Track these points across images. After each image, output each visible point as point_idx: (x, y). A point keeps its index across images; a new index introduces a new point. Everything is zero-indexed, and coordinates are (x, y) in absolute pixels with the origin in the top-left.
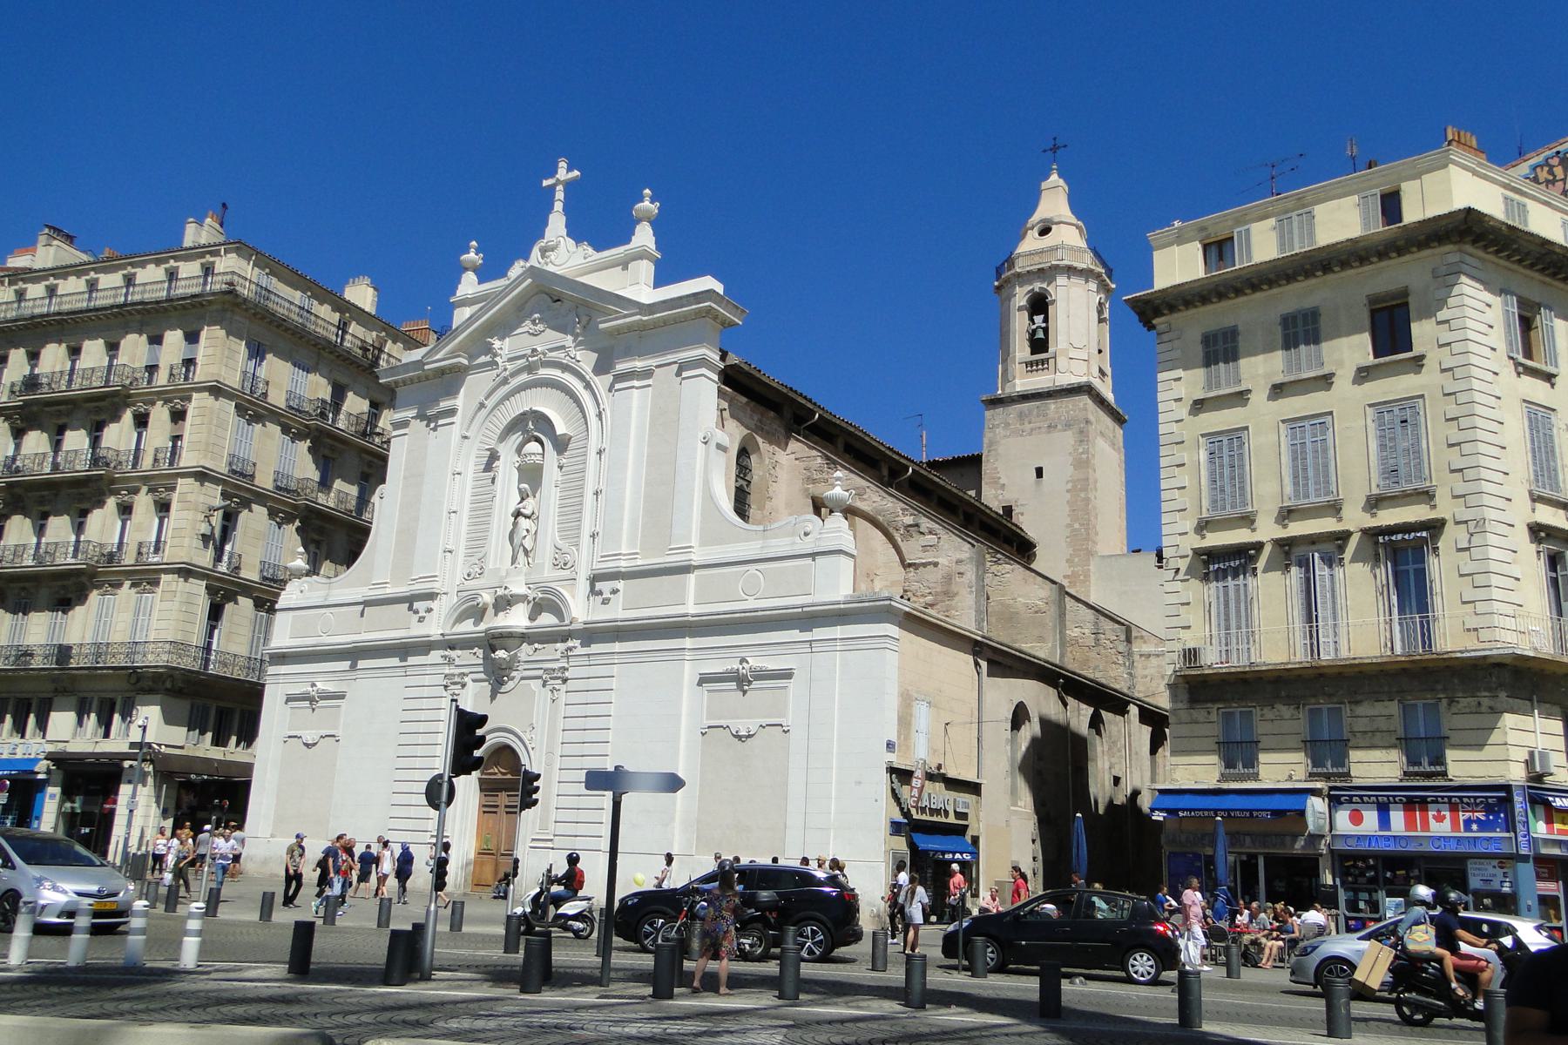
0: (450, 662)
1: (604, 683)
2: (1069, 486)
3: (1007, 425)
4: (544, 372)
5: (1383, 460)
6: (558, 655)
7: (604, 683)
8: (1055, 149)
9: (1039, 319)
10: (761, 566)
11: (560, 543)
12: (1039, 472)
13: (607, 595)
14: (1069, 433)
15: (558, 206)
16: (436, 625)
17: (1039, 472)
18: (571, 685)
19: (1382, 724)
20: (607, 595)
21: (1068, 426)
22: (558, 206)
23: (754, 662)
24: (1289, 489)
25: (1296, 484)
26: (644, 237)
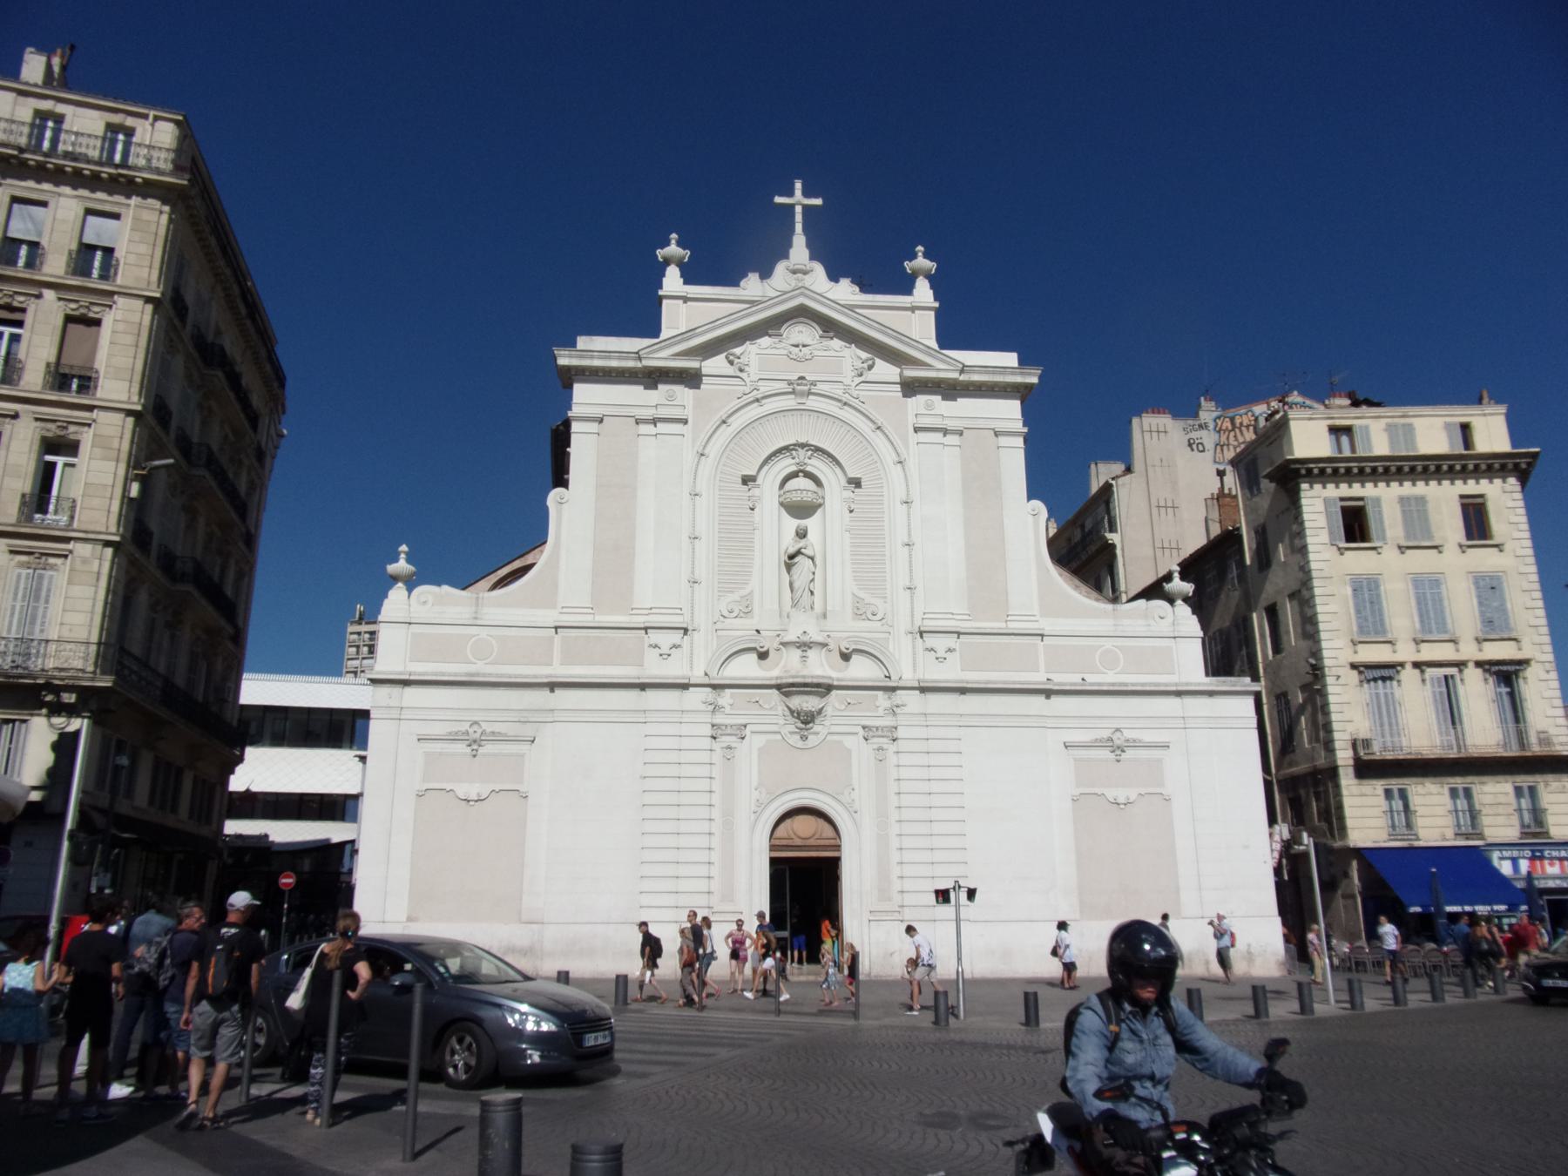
0: (716, 708)
1: (952, 746)
4: (813, 402)
5: (1482, 613)
6: (881, 712)
7: (952, 746)
10: (1120, 642)
11: (861, 594)
13: (941, 653)
15: (799, 227)
16: (694, 661)
19: (1502, 799)
22: (799, 227)
23: (1128, 734)
24: (1418, 625)
25: (1422, 622)
26: (923, 292)
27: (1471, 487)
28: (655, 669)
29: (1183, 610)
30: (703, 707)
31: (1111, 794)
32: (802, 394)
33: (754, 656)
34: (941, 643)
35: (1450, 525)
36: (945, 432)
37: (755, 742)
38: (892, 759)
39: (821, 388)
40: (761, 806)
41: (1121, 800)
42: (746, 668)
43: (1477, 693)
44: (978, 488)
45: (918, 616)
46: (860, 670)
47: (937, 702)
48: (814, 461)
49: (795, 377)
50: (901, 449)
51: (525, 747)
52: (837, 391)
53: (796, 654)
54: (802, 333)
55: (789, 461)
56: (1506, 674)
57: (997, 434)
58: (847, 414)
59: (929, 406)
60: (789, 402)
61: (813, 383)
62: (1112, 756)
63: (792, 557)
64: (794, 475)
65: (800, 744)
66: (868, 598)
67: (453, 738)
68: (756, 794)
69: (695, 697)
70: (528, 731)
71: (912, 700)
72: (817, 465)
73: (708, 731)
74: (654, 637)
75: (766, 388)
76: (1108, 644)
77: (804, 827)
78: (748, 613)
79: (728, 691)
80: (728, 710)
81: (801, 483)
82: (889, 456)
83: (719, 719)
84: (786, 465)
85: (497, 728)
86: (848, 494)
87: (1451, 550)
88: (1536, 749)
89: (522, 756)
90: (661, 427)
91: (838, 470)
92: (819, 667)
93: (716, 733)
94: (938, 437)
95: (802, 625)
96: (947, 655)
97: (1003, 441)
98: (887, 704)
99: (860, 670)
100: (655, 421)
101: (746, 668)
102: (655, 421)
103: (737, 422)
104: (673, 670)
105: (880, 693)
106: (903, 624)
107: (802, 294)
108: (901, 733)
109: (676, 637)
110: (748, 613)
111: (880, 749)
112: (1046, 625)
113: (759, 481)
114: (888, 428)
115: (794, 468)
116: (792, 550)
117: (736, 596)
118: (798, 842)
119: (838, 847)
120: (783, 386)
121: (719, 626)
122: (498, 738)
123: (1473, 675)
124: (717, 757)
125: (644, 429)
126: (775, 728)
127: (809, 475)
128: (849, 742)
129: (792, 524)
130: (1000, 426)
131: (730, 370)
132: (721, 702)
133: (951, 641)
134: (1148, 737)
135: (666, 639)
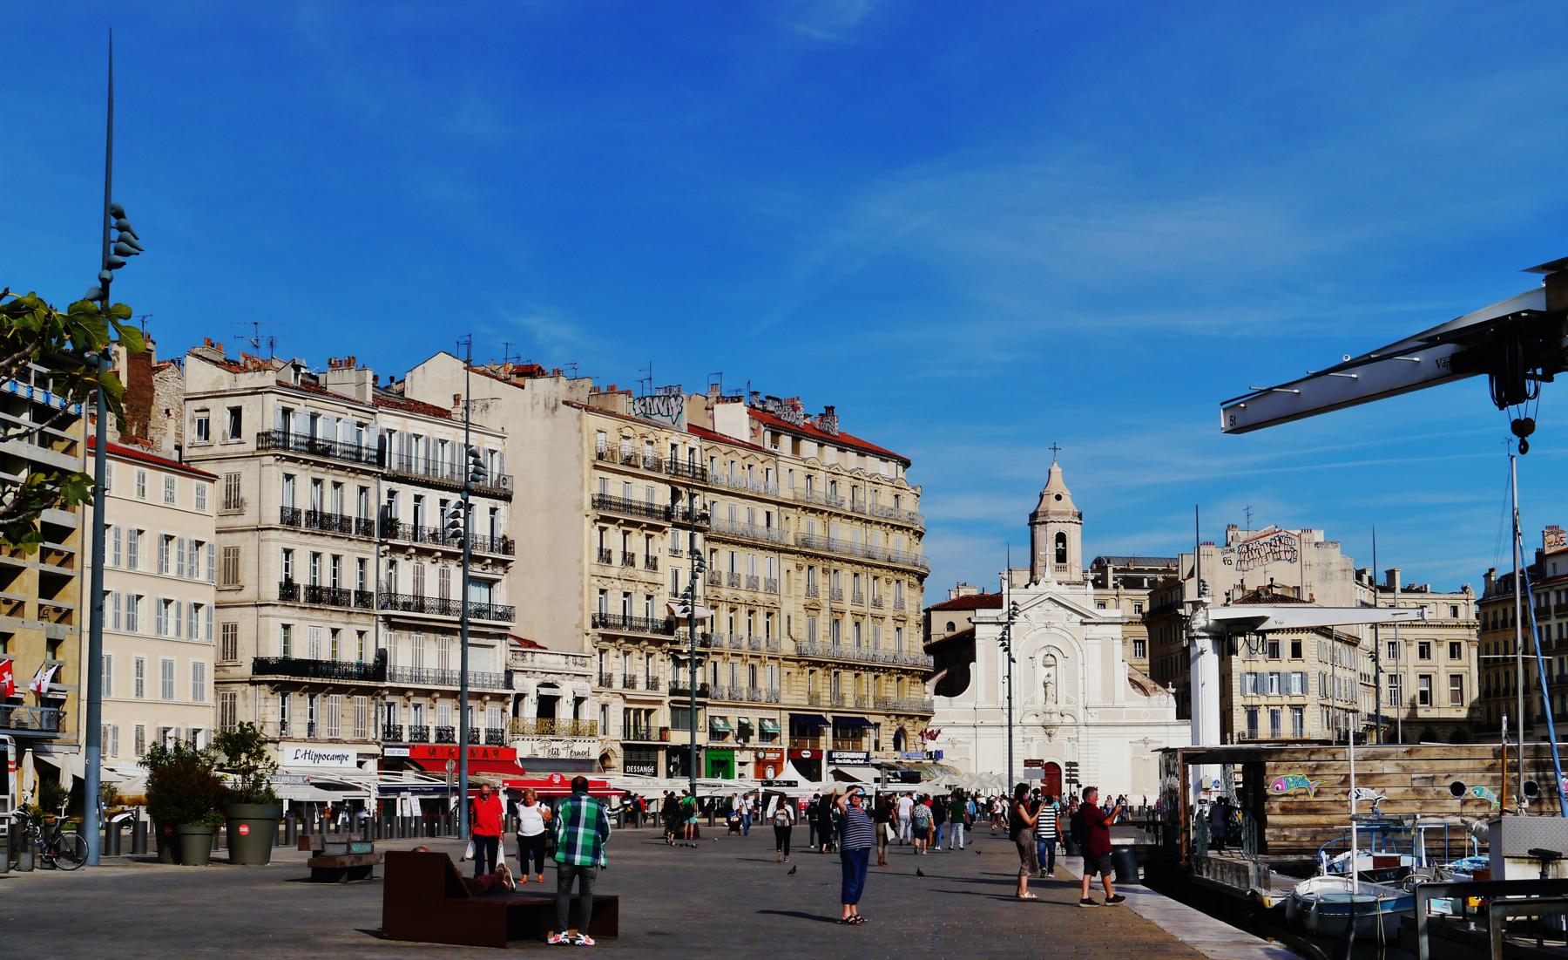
27: (1296, 636)
29: (1172, 698)
35: (1286, 650)
37: (1035, 743)
42: (1034, 720)
43: (1286, 717)
44: (1107, 659)
46: (1068, 720)
47: (1091, 730)
56: (1298, 709)
71: (1083, 729)
72: (1054, 652)
87: (1285, 661)
88: (1306, 736)
92: (1056, 719)
95: (1051, 706)
99: (1068, 720)
101: (1034, 720)
106: (1081, 705)
123: (1287, 709)
129: (1046, 671)
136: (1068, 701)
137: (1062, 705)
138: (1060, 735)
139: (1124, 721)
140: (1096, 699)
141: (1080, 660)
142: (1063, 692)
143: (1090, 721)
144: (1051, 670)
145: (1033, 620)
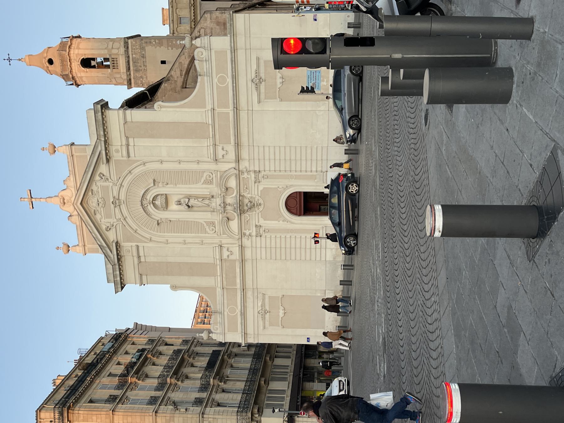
0: (250, 235)
2: (170, 48)
3: (142, 77)
4: (122, 197)
8: (9, 60)
9: (93, 63)
11: (202, 181)
12: (163, 62)
14: (146, 48)
17: (163, 62)
18: (262, 169)
20: (225, 152)
21: (143, 49)
23: (254, 75)
28: (236, 255)
30: (250, 240)
31: (279, 85)
32: (120, 202)
33: (231, 222)
34: (220, 153)
36: (128, 145)
37: (262, 222)
38: (267, 173)
39: (115, 194)
40: (285, 220)
41: (281, 80)
45: (209, 160)
46: (232, 183)
47: (245, 154)
48: (148, 198)
49: (112, 206)
50: (139, 163)
51: (267, 297)
52: (116, 189)
53: (228, 208)
54: (92, 203)
55: (149, 207)
57: (126, 122)
58: (125, 184)
59: (117, 151)
60: (123, 207)
61: (114, 197)
62: (263, 83)
63: (189, 206)
64: (154, 204)
65: (262, 206)
66: (204, 178)
67: (264, 319)
68: (281, 222)
69: (246, 242)
70: (260, 296)
71: (244, 165)
72: (150, 197)
73: (259, 238)
74: (225, 256)
75: (119, 216)
76: (215, 80)
77: (292, 203)
78: (213, 223)
79: (244, 231)
80: (251, 231)
81: (158, 202)
82: (142, 168)
83: (254, 234)
84: (151, 208)
85: (260, 304)
86: (160, 185)
89: (269, 297)
90: (141, 254)
91: (151, 189)
93: (259, 235)
94: (131, 148)
96: (225, 149)
97: (129, 119)
98: (246, 174)
99: (232, 183)
100: (139, 257)
102: (139, 257)
103: (135, 227)
104: (236, 250)
105: (241, 177)
106: (213, 166)
107: (76, 204)
108: (257, 169)
109: (225, 250)
110: (213, 223)
111: (263, 177)
112: (209, 107)
113: (158, 219)
114: (129, 169)
115: (152, 205)
116: (187, 207)
117: (207, 228)
118: (298, 205)
119: (300, 193)
120: (117, 210)
121: (219, 234)
122: (263, 305)
124: (268, 235)
125: (142, 259)
126: (257, 215)
127: (154, 199)
128: (261, 188)
130: (122, 122)
131: (113, 230)
132: (248, 233)
133: (219, 149)
134: (254, 67)
135: (225, 254)
136: (209, 182)
137: (215, 189)
138: (253, 192)
139: (230, 111)
140: (204, 147)
141: (157, 166)
142: (199, 189)
143: (232, 155)
144: (173, 200)
145: (112, 220)
